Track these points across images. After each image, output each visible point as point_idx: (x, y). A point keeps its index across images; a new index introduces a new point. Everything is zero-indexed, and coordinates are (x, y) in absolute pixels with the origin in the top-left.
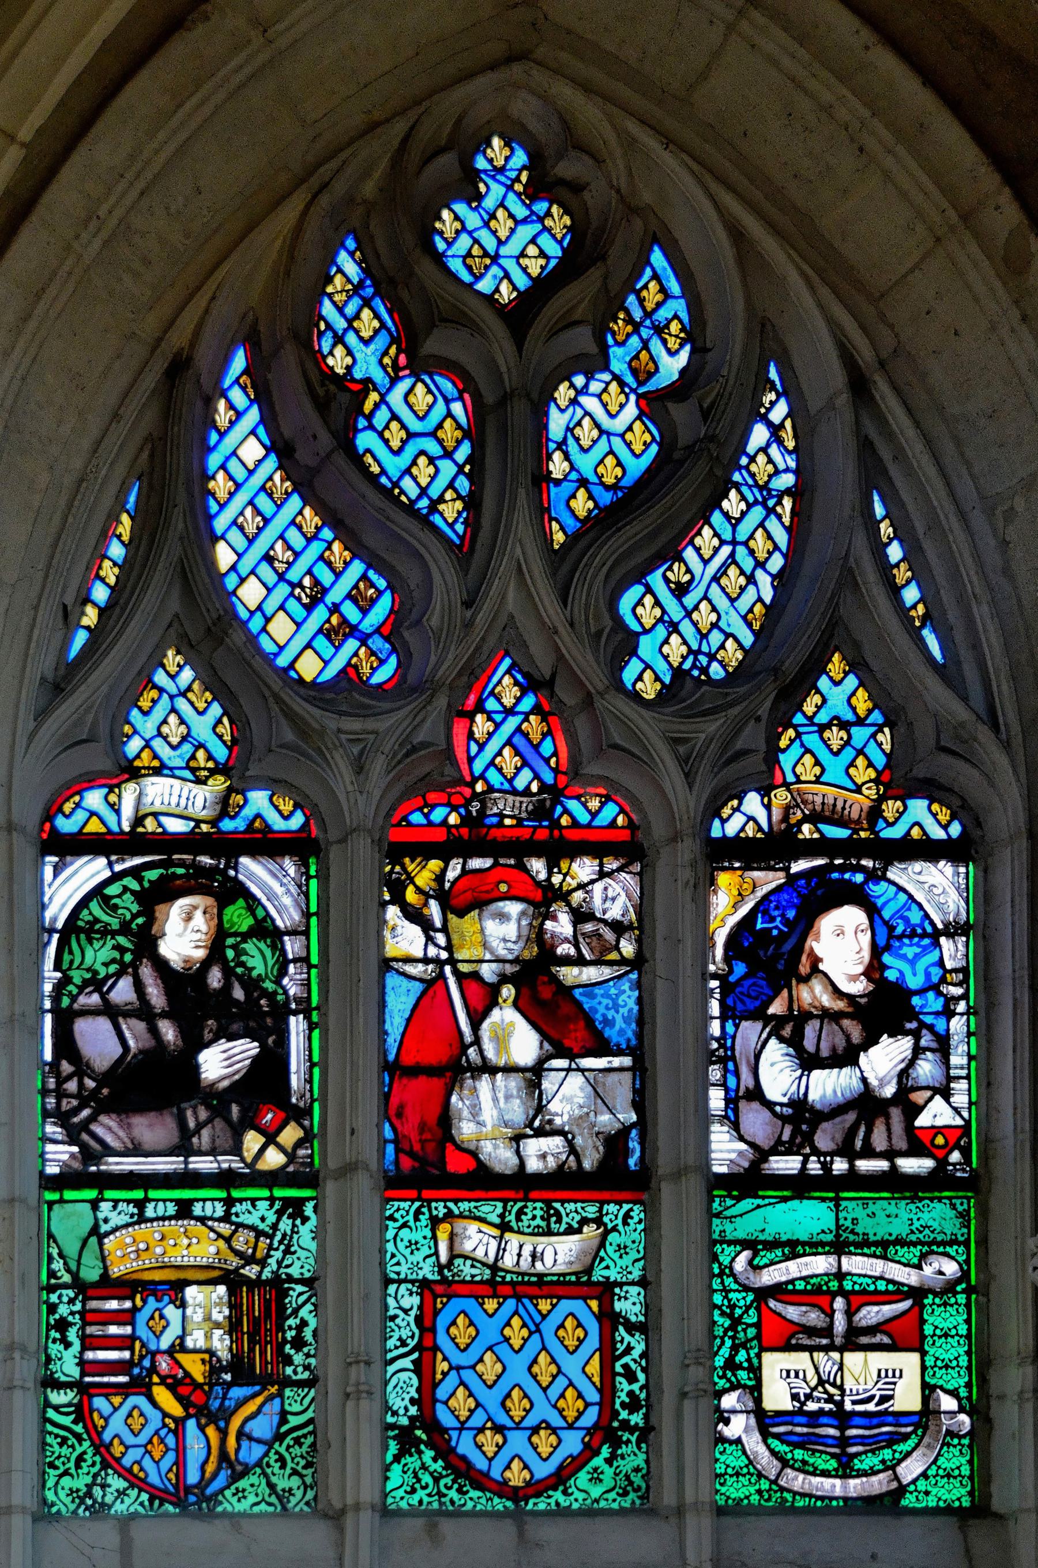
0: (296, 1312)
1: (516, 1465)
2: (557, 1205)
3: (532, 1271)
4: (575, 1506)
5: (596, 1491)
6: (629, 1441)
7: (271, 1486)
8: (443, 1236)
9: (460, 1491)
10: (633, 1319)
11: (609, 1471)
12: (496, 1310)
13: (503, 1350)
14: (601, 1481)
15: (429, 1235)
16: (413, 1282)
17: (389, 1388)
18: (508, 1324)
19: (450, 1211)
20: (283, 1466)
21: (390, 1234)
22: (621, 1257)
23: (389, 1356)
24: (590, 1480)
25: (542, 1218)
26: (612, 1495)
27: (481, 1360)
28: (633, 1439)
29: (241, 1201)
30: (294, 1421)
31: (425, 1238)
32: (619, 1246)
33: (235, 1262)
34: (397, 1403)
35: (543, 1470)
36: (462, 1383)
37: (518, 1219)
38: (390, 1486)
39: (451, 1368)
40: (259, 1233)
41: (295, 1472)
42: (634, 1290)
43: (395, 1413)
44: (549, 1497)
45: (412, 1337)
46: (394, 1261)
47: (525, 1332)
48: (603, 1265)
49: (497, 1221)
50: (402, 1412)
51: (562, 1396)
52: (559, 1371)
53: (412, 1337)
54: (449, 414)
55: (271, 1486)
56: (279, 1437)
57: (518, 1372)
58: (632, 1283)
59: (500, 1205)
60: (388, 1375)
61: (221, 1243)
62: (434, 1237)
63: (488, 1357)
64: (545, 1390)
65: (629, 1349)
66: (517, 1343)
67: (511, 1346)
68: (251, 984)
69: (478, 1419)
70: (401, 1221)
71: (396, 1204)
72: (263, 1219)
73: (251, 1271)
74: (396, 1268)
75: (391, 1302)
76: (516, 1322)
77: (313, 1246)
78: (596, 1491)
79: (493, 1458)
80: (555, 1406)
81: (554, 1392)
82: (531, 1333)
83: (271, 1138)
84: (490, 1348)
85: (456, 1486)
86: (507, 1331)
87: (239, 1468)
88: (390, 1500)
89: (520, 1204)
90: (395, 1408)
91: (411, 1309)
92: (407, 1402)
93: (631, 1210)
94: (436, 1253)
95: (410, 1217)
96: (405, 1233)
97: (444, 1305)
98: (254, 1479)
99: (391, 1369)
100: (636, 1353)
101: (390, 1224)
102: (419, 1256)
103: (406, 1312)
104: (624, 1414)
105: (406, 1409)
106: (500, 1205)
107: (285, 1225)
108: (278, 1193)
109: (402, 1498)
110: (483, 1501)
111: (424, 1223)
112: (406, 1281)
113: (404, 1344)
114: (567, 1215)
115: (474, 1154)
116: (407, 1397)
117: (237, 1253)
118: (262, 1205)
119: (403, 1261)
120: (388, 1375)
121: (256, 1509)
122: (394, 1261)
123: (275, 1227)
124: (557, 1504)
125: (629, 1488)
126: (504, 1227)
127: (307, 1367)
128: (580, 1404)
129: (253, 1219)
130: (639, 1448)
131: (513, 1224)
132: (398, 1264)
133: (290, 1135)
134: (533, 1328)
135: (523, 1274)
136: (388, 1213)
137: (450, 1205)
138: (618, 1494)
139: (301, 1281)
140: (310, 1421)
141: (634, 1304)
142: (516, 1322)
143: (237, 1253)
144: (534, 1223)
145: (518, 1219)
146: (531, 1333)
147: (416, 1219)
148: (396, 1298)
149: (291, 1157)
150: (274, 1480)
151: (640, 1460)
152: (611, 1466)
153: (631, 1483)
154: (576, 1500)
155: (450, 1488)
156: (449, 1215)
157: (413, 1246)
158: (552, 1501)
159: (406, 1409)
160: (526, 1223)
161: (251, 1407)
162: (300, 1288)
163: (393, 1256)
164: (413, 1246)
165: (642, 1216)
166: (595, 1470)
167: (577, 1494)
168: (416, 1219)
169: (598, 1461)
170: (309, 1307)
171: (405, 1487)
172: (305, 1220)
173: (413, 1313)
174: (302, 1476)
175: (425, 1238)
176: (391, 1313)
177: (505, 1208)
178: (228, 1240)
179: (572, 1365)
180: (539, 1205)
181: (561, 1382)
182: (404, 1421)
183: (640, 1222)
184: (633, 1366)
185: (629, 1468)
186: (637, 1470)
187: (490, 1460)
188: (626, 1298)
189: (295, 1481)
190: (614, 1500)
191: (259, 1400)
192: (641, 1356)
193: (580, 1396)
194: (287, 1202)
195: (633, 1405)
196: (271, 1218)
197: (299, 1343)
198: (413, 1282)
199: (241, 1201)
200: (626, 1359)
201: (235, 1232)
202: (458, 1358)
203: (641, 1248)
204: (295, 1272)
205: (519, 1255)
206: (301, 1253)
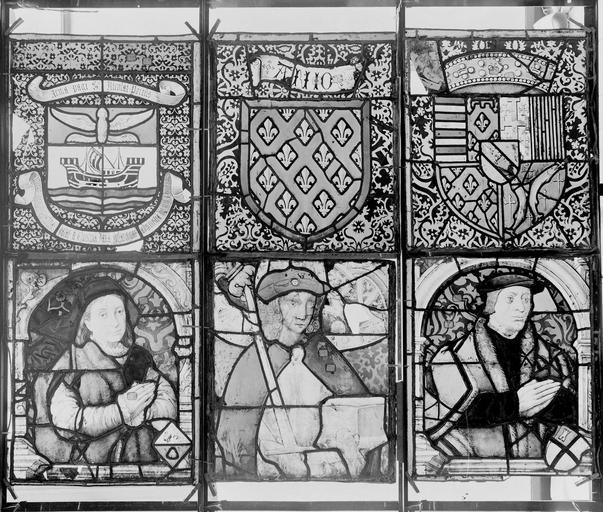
1: (305, 220)
2: (332, 46)
3: (316, 91)
4: (345, 248)
5: (359, 237)
6: (382, 204)
8: (255, 67)
9: (265, 237)
10: (385, 121)
11: (368, 225)
12: (291, 117)
13: (295, 144)
14: (362, 231)
15: (246, 68)
16: (234, 98)
17: (219, 169)
18: (299, 126)
19: (259, 49)
21: (219, 67)
22: (376, 80)
23: (218, 148)
24: (355, 230)
25: (322, 55)
26: (370, 241)
27: (281, 150)
28: (385, 203)
31: (243, 69)
32: (374, 72)
34: (224, 180)
35: (323, 223)
36: (268, 165)
37: (306, 56)
38: (218, 233)
39: (261, 156)
42: (385, 102)
43: (223, 186)
44: (328, 241)
45: (234, 135)
46: (221, 85)
47: (311, 132)
48: (364, 85)
49: (293, 57)
50: (227, 185)
51: (336, 174)
52: (335, 157)
53: (234, 135)
57: (305, 154)
58: (385, 98)
59: (293, 46)
60: (218, 160)
62: (249, 69)
63: (286, 148)
64: (324, 170)
65: (382, 142)
66: (305, 139)
67: (301, 141)
70: (227, 58)
71: (224, 47)
74: (223, 90)
75: (220, 111)
76: (305, 125)
78: (359, 237)
79: (289, 216)
80: (331, 182)
81: (330, 172)
82: (315, 133)
84: (287, 142)
85: (263, 234)
86: (299, 131)
88: (218, 243)
89: (307, 46)
90: (222, 182)
91: (234, 116)
92: (230, 178)
93: (383, 48)
94: (250, 80)
95: (233, 56)
96: (229, 66)
97: (256, 114)
99: (220, 157)
100: (386, 145)
101: (220, 60)
102: (239, 82)
103: (230, 118)
104: (378, 186)
105: (230, 183)
106: (293, 46)
109: (226, 242)
110: (281, 243)
111: (242, 59)
112: (230, 97)
113: (229, 140)
114: (339, 53)
116: (231, 175)
119: (228, 84)
120: (218, 160)
122: (221, 85)
124: (333, 246)
125: (382, 236)
128: (349, 180)
130: (389, 209)
131: (303, 59)
132: (225, 86)
134: (316, 129)
135: (309, 93)
136: (218, 52)
137: (260, 46)
138: (374, 239)
141: (385, 111)
142: (305, 125)
144: (316, 59)
145: (306, 56)
146: (315, 133)
147: (238, 57)
148: (223, 109)
151: (389, 216)
152: (369, 221)
153: (383, 232)
154: (346, 244)
155: (259, 235)
157: (235, 75)
158: (329, 244)
159: (230, 183)
160: (311, 59)
163: (222, 81)
164: (235, 75)
165: (390, 52)
166: (359, 223)
167: (347, 240)
168: (238, 57)
169: (361, 218)
171: (228, 234)
173: (234, 119)
175: (243, 69)
176: (220, 119)
177: (297, 47)
179: (343, 154)
180: (319, 46)
181: (335, 165)
182: (229, 191)
183: (388, 56)
184: (384, 153)
185: (381, 222)
186: (387, 223)
187: (287, 217)
188: (380, 108)
190: (372, 244)
192: (390, 147)
193: (348, 174)
195: (385, 180)
198: (234, 98)
200: (380, 149)
202: (265, 150)
203: (389, 74)
205: (306, 80)
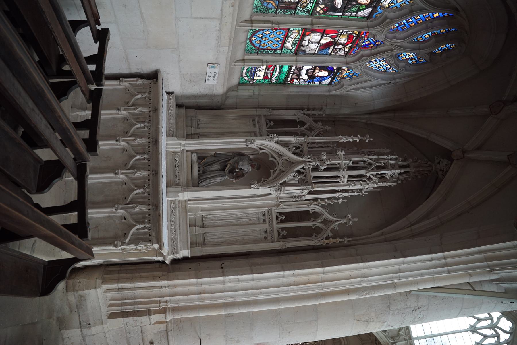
0: (289, 11)
7: (258, 7)
20: (262, 9)
29: (313, 5)
30: (270, 11)
33: (301, 3)
35: (253, 42)
40: (305, 7)
41: (260, 10)
54: (422, 39)
55: (258, 7)
56: (267, 8)
61: (306, 1)
68: (350, 8)
69: (264, 34)
72: (308, 8)
73: (299, 5)
77: (301, 14)
83: (322, 9)
87: (263, 2)
98: (260, 4)
107: (306, 11)
108: (312, 10)
115: (309, 35)
117: (303, 3)
118: (311, 8)
121: (255, 5)
123: (306, 9)
126: (295, 38)
127: (279, 13)
129: (308, 6)
133: (322, 12)
139: (295, 12)
140: (269, 13)
143: (303, 3)
149: (318, 12)
150: (260, 7)
156: (299, 32)
161: (274, 4)
162: (294, 12)
170: (290, 13)
172: (306, 14)
174: (259, 11)
178: (306, 2)
179: (270, 45)
189: (258, 10)
191: (275, 5)
194: (310, 11)
196: (308, 9)
197: (284, 12)
199: (313, 5)
201: (307, 3)
204: (297, 12)
206: (300, 12)
